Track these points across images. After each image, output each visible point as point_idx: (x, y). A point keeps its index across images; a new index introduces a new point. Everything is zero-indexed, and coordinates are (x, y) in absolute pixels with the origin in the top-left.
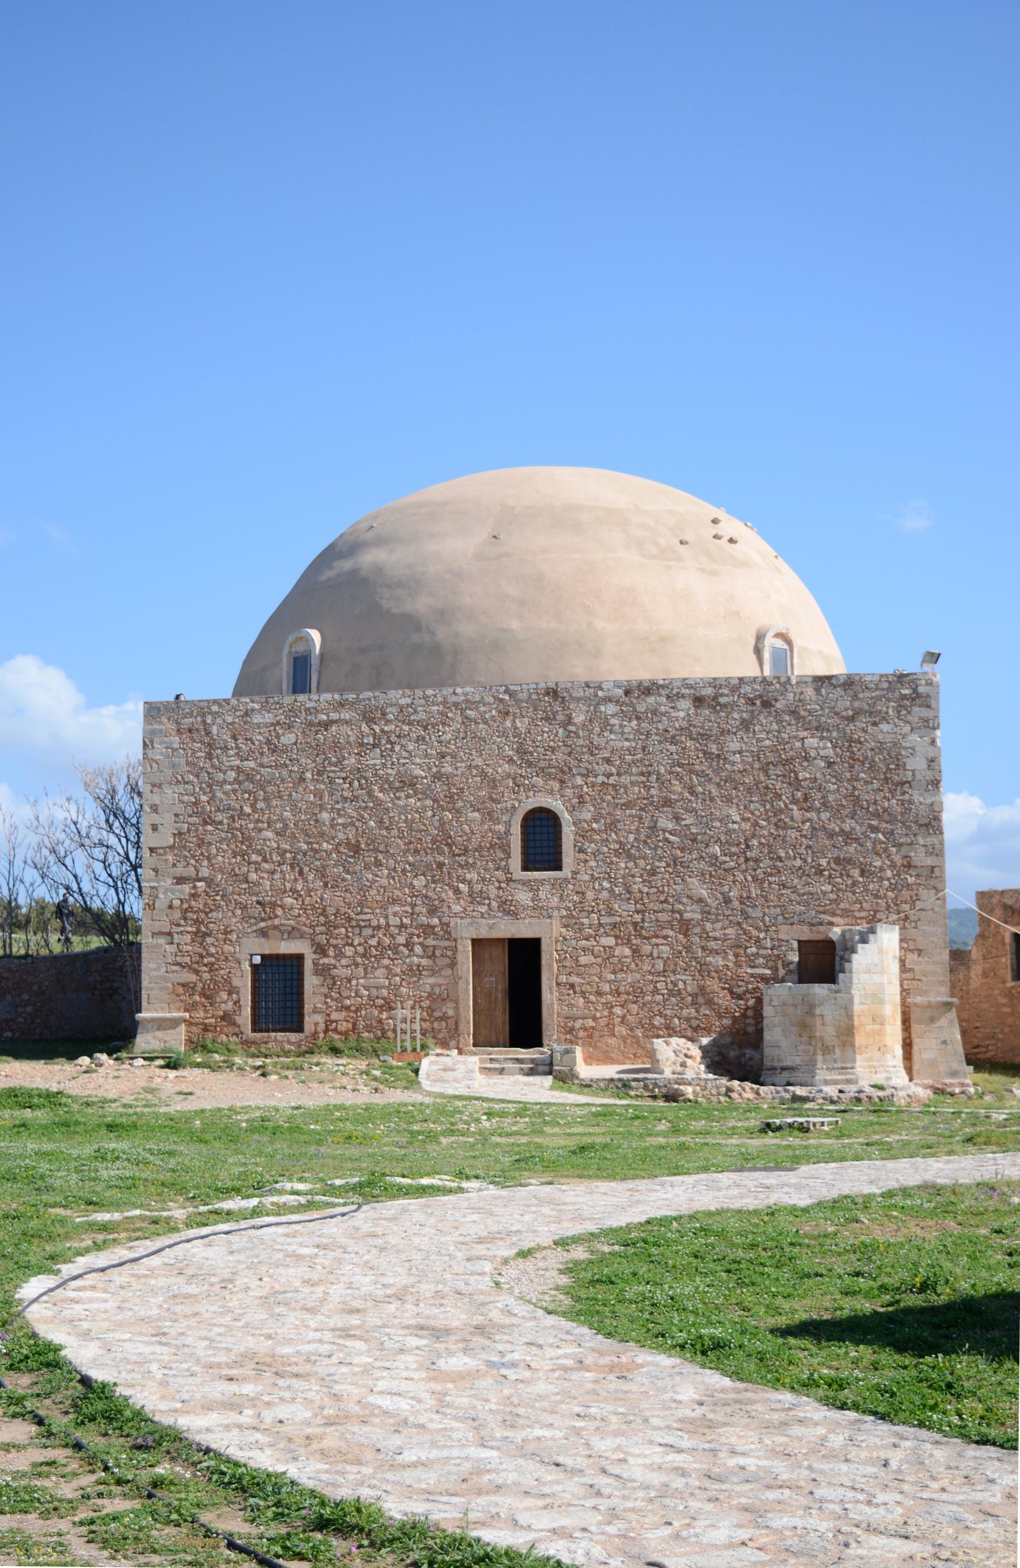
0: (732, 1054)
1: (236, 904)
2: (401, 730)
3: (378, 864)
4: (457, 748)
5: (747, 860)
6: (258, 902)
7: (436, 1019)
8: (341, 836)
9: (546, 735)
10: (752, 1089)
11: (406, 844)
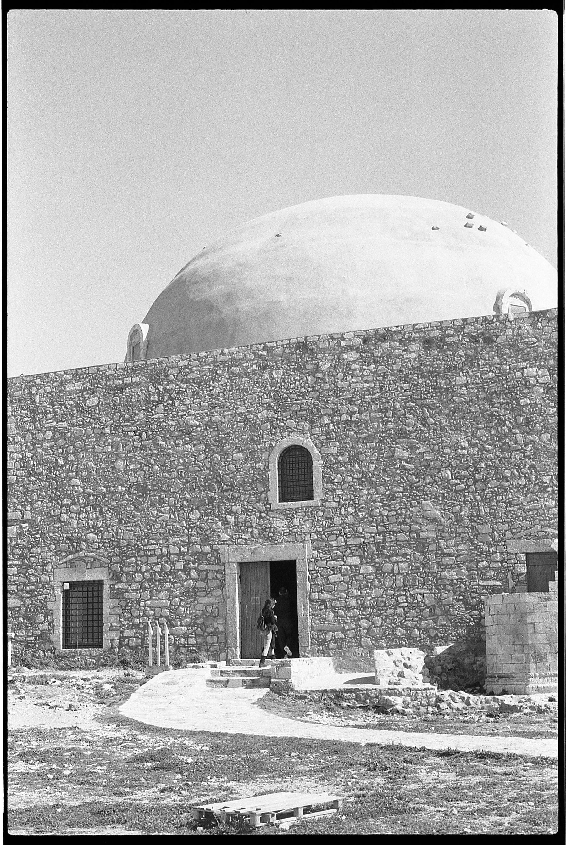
0: (467, 661)
1: (51, 540)
2: (180, 387)
3: (162, 502)
4: (225, 399)
5: (476, 481)
6: (68, 538)
7: (209, 634)
8: (132, 479)
9: (297, 383)
10: (462, 698)
11: (184, 484)
